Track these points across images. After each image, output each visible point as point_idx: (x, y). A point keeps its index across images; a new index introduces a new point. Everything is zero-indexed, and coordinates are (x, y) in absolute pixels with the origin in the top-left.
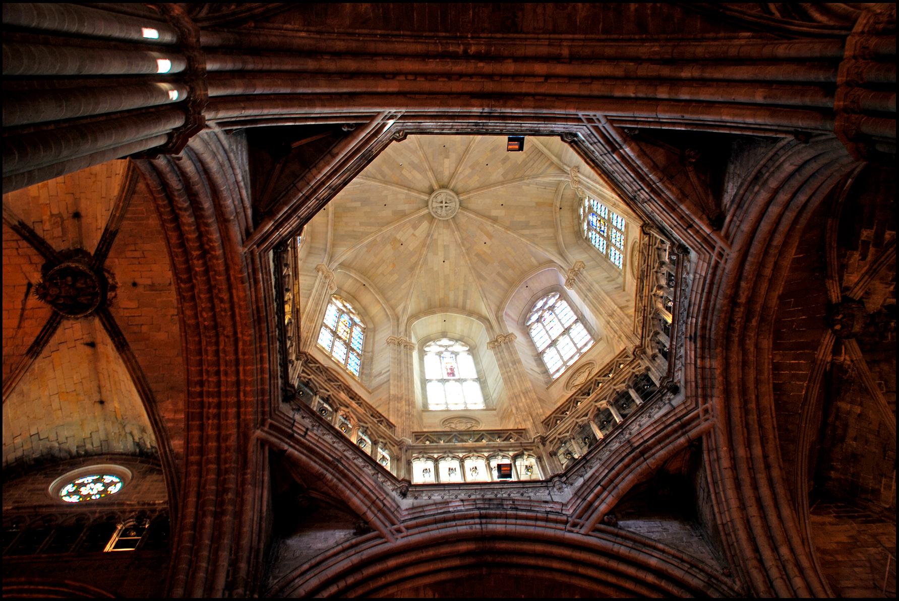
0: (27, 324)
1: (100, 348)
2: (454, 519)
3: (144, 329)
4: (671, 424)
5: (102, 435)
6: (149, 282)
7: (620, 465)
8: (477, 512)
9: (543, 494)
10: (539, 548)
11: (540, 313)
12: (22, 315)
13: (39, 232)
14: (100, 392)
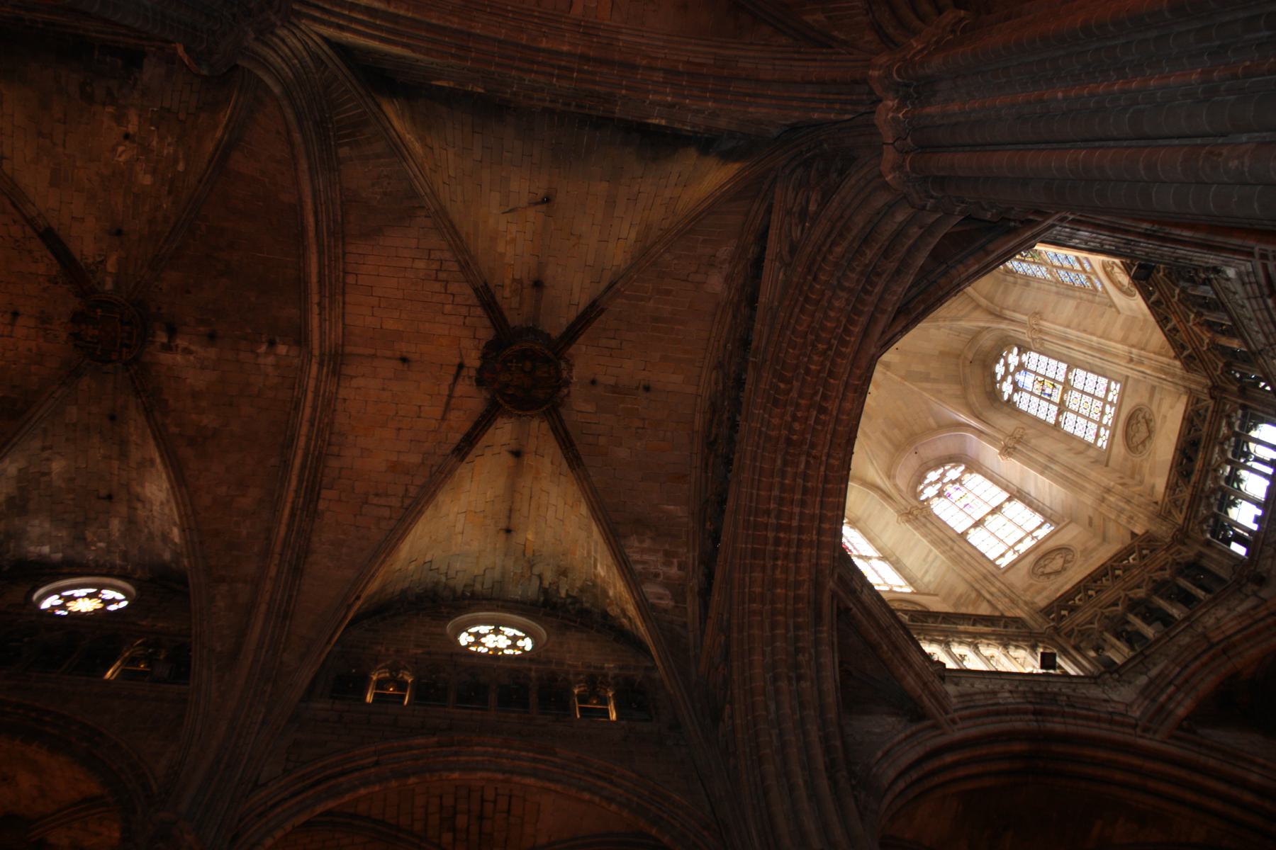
0: (453, 415)
1: (529, 460)
2: (1007, 713)
3: (602, 441)
4: (1262, 619)
5: (497, 574)
6: (612, 381)
7: (1198, 663)
8: (1030, 707)
9: (1095, 692)
10: (1102, 754)
11: (939, 485)
12: (448, 403)
13: (498, 298)
14: (509, 517)
